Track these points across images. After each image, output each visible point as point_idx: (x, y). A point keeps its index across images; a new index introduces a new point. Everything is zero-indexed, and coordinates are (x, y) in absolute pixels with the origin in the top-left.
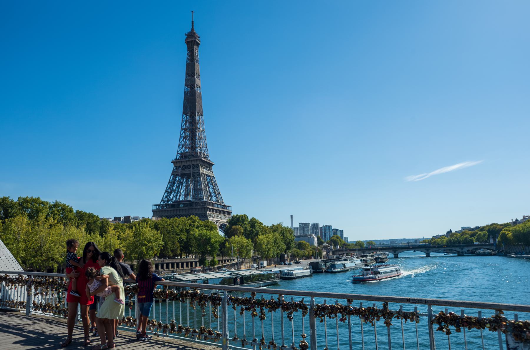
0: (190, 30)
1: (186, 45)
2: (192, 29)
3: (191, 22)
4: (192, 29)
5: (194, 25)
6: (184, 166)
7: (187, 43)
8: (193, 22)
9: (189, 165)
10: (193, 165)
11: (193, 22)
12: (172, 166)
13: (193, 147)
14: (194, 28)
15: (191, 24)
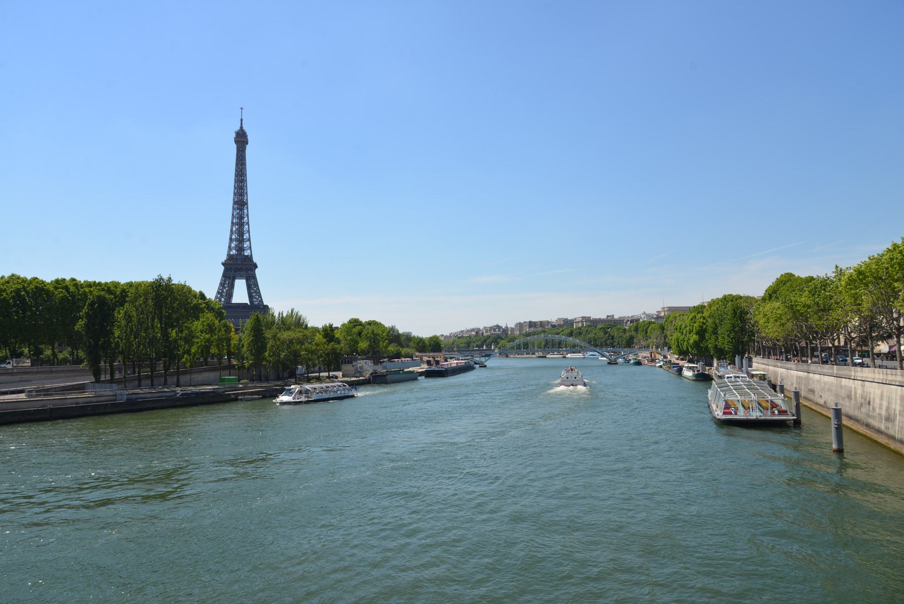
0: (238, 128)
1: (235, 146)
2: (241, 127)
3: (240, 120)
4: (241, 127)
5: (243, 122)
6: (236, 268)
7: (236, 142)
8: (242, 120)
9: (242, 268)
10: (246, 268)
11: (242, 120)
12: (223, 268)
13: (240, 249)
14: (243, 126)
15: (240, 122)
